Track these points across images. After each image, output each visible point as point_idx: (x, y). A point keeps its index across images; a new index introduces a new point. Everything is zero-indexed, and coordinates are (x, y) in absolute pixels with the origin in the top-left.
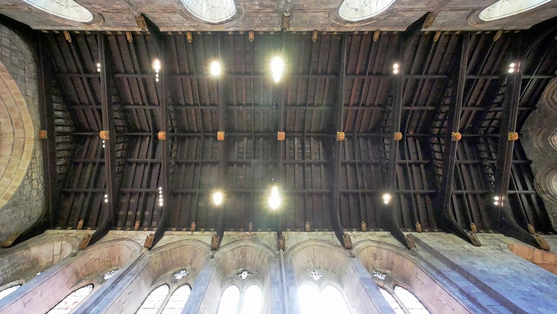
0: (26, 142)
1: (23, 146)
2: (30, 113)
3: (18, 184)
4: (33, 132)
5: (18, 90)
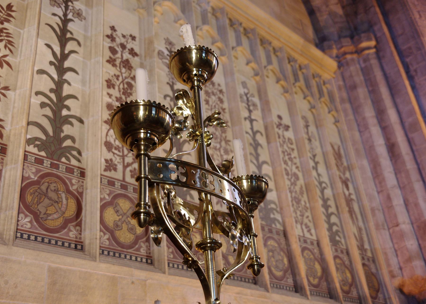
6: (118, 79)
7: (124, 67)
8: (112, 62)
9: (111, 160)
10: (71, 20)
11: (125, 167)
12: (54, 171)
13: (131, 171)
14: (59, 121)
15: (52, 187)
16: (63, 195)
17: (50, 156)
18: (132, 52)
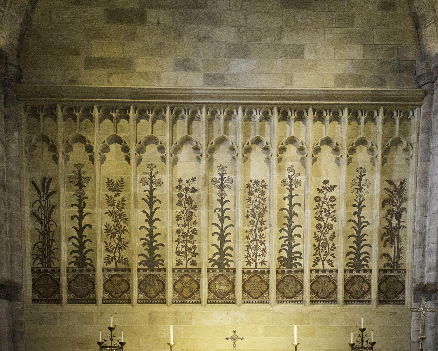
6: (183, 213)
7: (187, 203)
8: (179, 204)
9: (179, 260)
11: (187, 261)
12: (152, 273)
13: (190, 262)
15: (151, 280)
16: (156, 282)
17: (149, 267)
18: (194, 190)
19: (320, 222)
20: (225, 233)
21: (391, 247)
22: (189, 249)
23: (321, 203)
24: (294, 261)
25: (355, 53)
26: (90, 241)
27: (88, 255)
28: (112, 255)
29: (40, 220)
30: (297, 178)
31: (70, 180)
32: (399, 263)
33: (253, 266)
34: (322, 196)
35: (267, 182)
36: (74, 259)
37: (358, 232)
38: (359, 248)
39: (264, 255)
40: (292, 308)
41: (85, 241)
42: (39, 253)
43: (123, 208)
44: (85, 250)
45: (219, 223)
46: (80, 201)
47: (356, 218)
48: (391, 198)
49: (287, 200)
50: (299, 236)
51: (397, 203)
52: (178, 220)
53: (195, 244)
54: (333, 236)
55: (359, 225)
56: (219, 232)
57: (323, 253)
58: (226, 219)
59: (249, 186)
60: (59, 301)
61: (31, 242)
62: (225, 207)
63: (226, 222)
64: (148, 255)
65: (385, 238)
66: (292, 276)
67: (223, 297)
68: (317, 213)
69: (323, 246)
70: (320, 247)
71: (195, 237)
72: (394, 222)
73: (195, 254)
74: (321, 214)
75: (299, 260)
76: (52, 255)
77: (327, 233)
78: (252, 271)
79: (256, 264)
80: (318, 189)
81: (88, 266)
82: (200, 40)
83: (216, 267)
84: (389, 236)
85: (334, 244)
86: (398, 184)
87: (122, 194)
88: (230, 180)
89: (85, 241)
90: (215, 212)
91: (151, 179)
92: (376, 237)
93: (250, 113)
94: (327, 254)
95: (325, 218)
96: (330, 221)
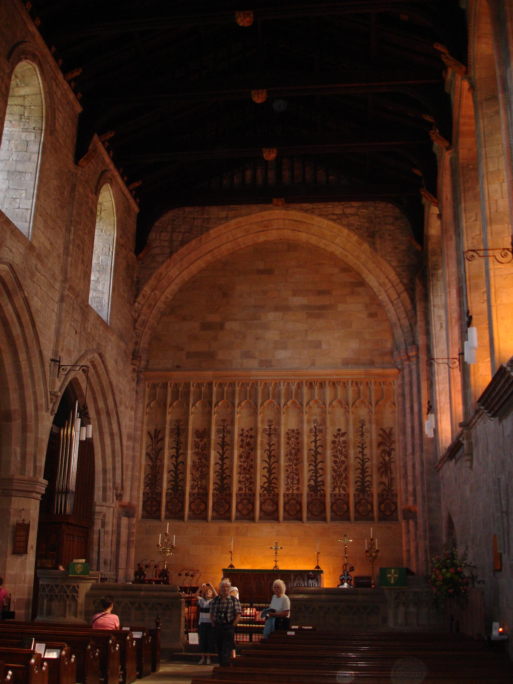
0: (290, 218)
1: (296, 221)
2: (251, 214)
3: (346, 231)
4: (276, 211)
5: (221, 227)
8: (242, 446)
10: (226, 436)
11: (246, 488)
14: (222, 479)
18: (251, 437)
19: (336, 459)
20: (272, 467)
21: (386, 477)
22: (247, 479)
23: (336, 445)
24: (319, 488)
25: (354, 344)
26: (183, 473)
27: (180, 484)
28: (196, 483)
29: (151, 458)
30: (320, 427)
31: (172, 431)
32: (392, 488)
33: (291, 492)
34: (337, 440)
35: (300, 431)
36: (171, 487)
37: (363, 465)
38: (364, 478)
39: (298, 484)
40: (319, 525)
41: (179, 473)
42: (149, 482)
43: (205, 450)
44: (178, 480)
45: (267, 460)
46: (177, 445)
47: (360, 456)
48: (384, 441)
49: (313, 443)
50: (322, 469)
51: (388, 444)
52: (240, 458)
53: (252, 475)
54: (346, 469)
55: (363, 460)
56: (268, 466)
57: (339, 482)
58: (273, 457)
59: (288, 434)
60: (159, 518)
61: (145, 474)
62: (272, 448)
63: (273, 460)
64: (220, 484)
65: (382, 470)
66: (318, 499)
67: (271, 516)
68: (334, 453)
69: (340, 476)
70: (337, 478)
71: (252, 470)
72: (387, 458)
73: (251, 483)
74: (337, 453)
75: (322, 487)
76: (157, 483)
77: (341, 467)
78: (290, 495)
79: (293, 490)
80: (334, 435)
81: (180, 491)
82: (257, 339)
83: (265, 492)
84: (384, 469)
85: (346, 475)
86: (388, 431)
87: (205, 440)
88: (275, 430)
89: (179, 473)
90: (265, 452)
91: (223, 429)
92: (375, 469)
93: (288, 384)
94: (341, 483)
95: (340, 456)
96: (343, 458)
